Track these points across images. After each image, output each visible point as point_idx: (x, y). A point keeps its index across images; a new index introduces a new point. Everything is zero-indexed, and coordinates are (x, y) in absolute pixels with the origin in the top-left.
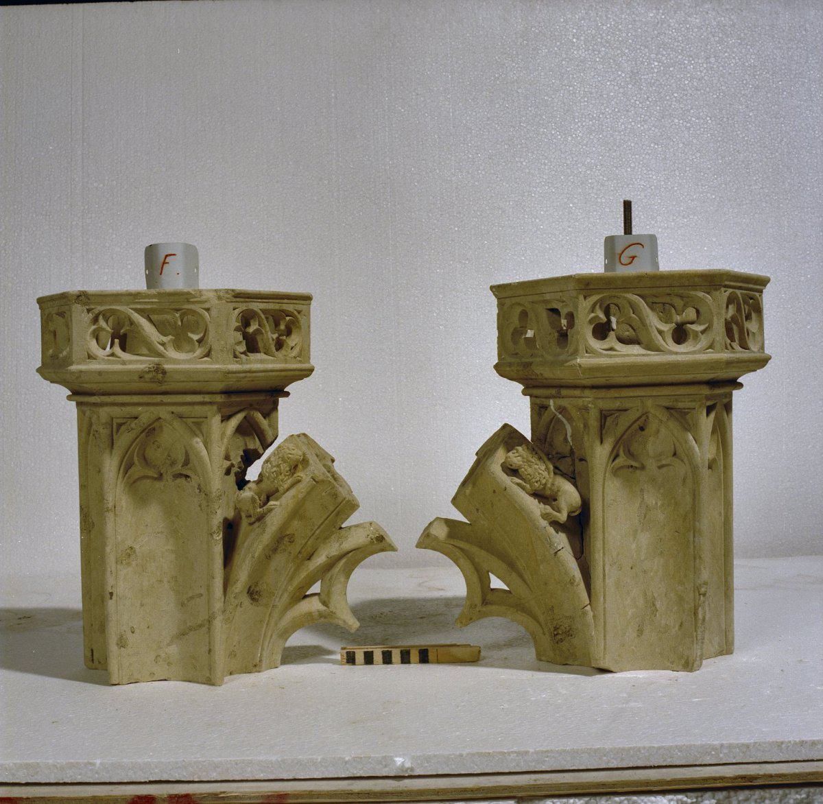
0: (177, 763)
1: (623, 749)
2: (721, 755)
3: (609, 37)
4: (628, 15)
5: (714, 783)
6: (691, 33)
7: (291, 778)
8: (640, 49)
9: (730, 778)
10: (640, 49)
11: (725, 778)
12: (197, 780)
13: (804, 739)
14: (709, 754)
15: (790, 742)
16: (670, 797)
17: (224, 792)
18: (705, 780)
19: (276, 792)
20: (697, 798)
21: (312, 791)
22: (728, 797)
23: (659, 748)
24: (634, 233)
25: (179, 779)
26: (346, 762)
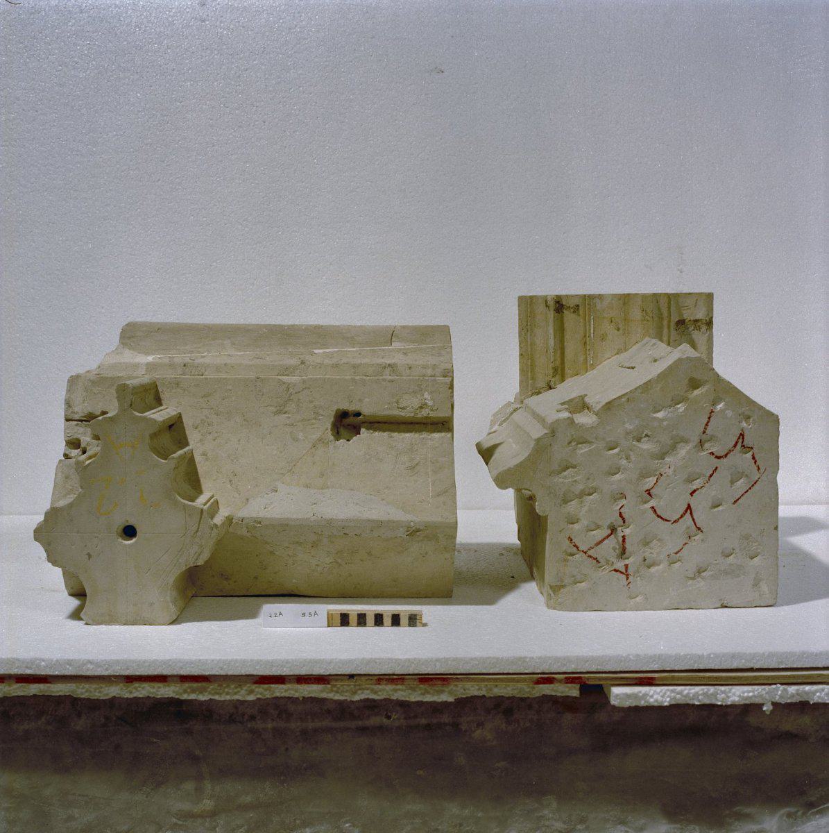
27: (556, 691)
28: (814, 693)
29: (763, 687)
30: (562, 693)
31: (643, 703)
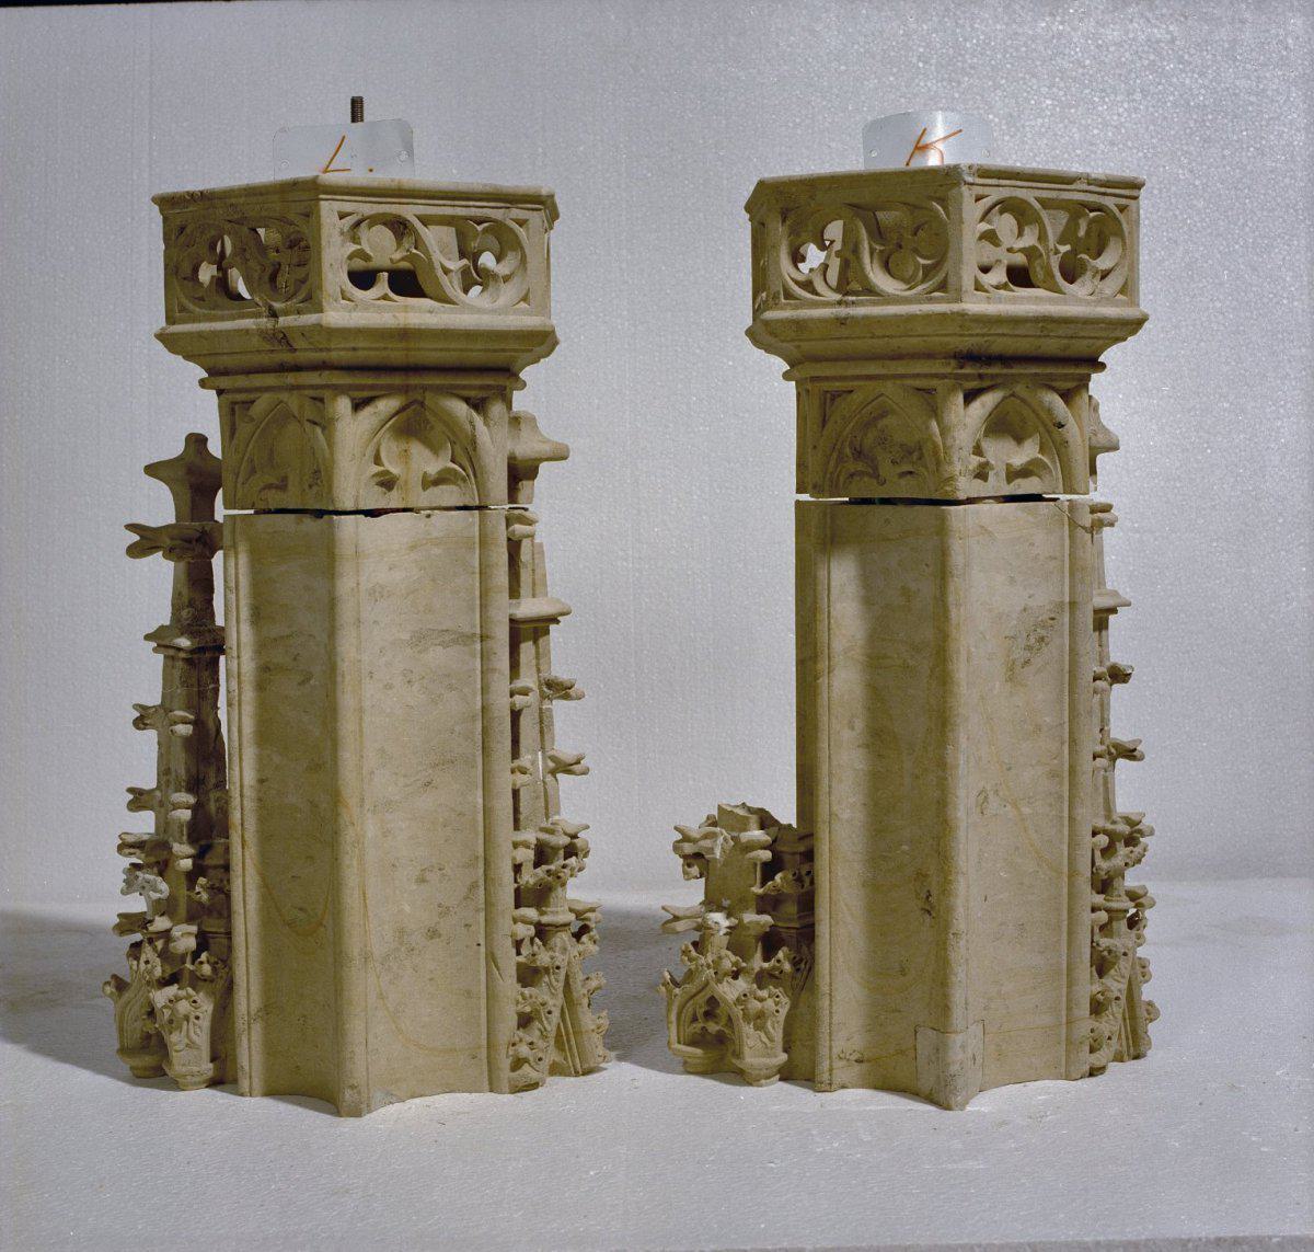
3: (975, 60)
4: (1007, 24)
6: (1105, 53)
8: (1024, 79)
10: (1024, 79)
13: (1222, 1235)
15: (1200, 1239)
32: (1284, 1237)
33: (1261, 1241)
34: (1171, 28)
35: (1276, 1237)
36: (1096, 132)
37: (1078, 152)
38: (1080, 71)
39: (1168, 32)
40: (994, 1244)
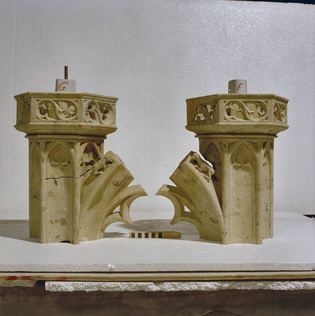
0: (26, 264)
1: (195, 264)
2: (232, 267)
5: (228, 278)
7: (69, 271)
9: (234, 276)
11: (232, 276)
12: (34, 271)
14: (227, 267)
15: (258, 263)
16: (211, 283)
17: (43, 276)
18: (225, 277)
19: (62, 276)
20: (222, 283)
21: (76, 276)
22: (234, 284)
23: (208, 264)
24: (68, 79)
25: (27, 271)
26: (91, 266)
27: (22, 284)
28: (146, 286)
29: (121, 283)
30: (25, 285)
31: (59, 290)
32: (279, 263)
33: (273, 264)
34: (262, 10)
35: (276, 263)
36: (244, 33)
37: (240, 38)
38: (241, 19)
39: (262, 11)
40: (207, 264)
